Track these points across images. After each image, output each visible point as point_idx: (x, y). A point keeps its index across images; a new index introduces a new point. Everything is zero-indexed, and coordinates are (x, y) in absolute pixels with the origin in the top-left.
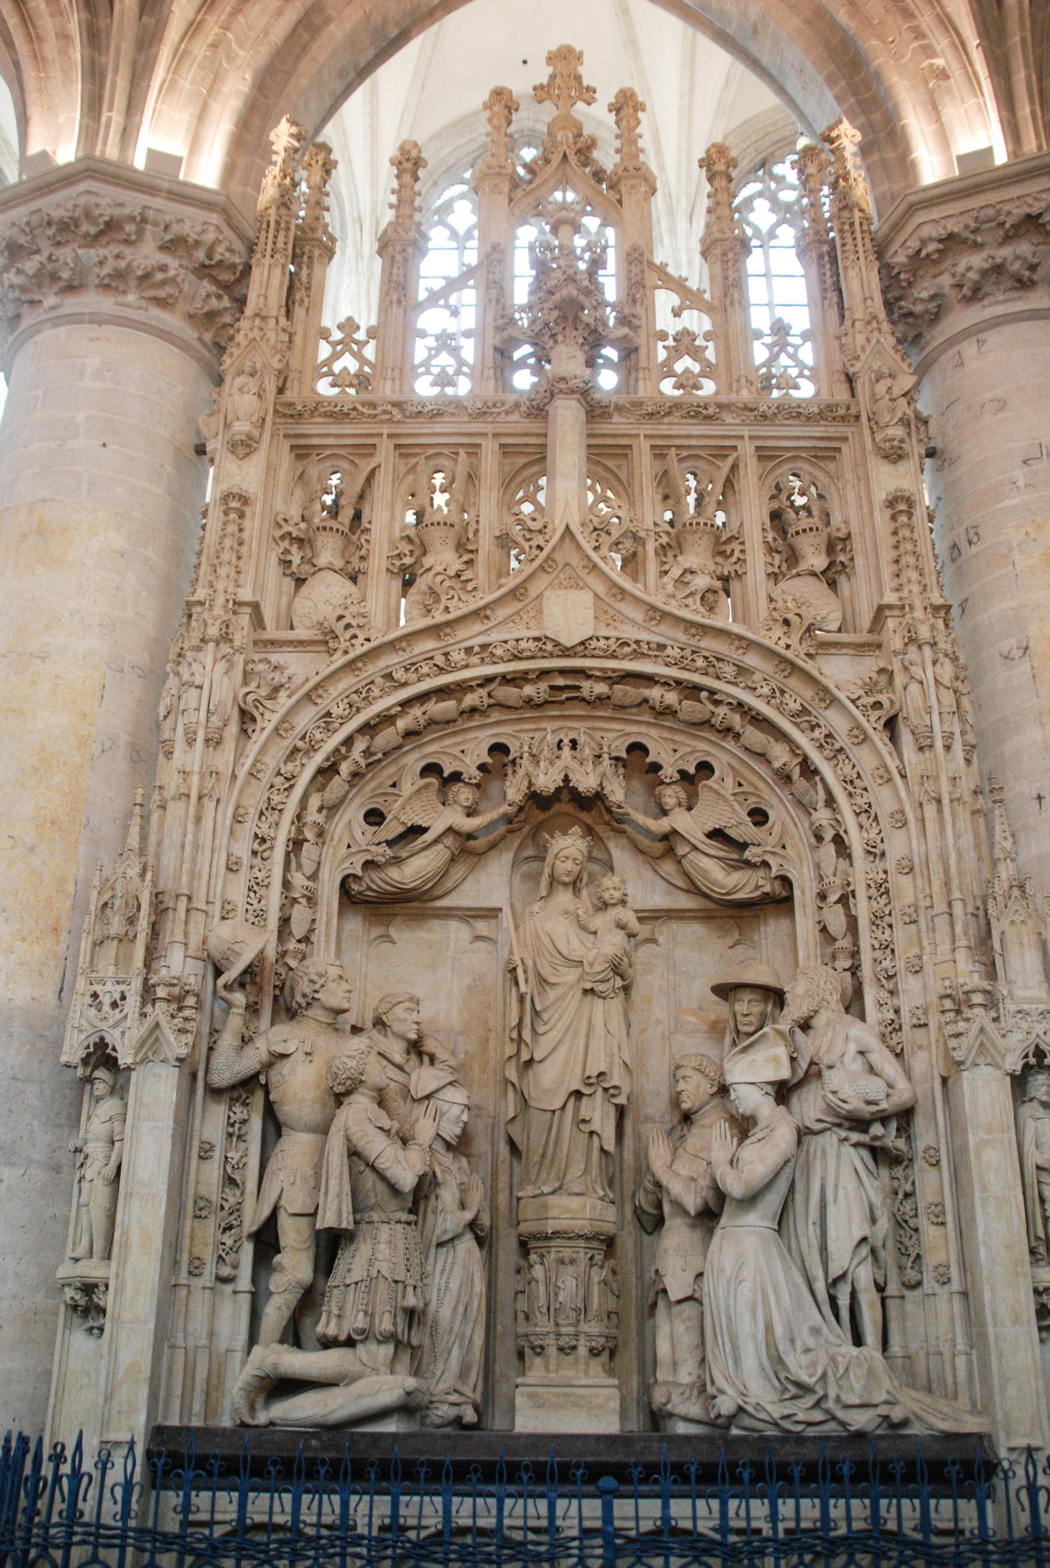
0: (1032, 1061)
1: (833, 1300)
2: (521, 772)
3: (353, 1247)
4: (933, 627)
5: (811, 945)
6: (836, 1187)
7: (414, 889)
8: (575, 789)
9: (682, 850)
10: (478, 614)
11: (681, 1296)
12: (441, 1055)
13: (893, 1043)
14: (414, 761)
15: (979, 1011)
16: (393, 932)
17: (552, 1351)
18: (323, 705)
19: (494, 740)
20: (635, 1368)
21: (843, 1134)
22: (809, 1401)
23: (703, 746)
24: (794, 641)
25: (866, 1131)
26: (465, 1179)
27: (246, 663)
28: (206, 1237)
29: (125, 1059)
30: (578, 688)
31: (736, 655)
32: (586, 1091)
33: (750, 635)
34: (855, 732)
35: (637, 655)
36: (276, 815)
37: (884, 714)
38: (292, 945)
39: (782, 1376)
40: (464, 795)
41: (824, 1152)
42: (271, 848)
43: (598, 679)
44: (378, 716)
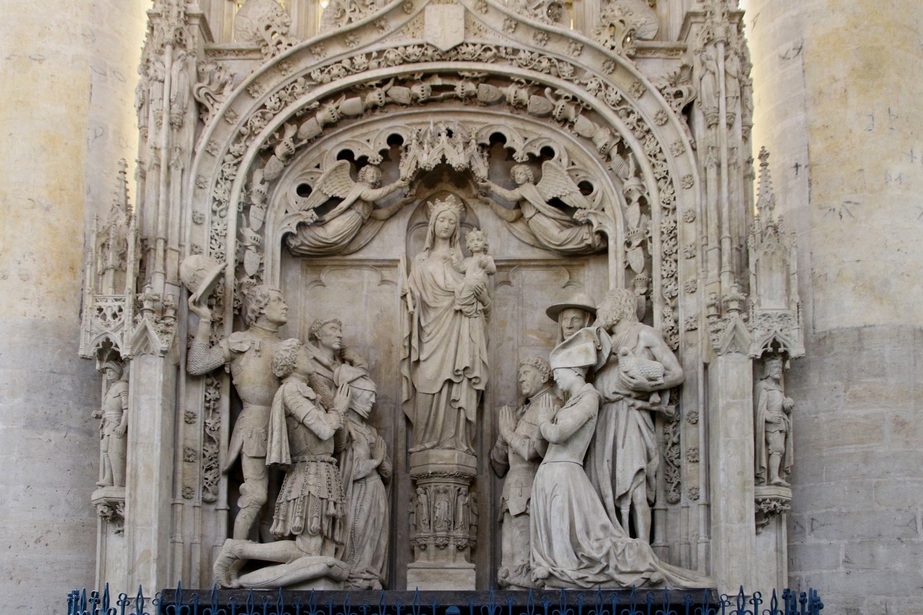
4: (727, 30)
5: (620, 279)
10: (374, 24)
11: (518, 512)
17: (432, 548)
18: (259, 98)
20: (488, 560)
24: (618, 43)
26: (374, 440)
27: (198, 64)
30: (452, 88)
31: (572, 57)
33: (584, 38)
34: (660, 116)
35: (497, 59)
37: (683, 101)
38: (245, 279)
41: (617, 414)
42: (227, 209)
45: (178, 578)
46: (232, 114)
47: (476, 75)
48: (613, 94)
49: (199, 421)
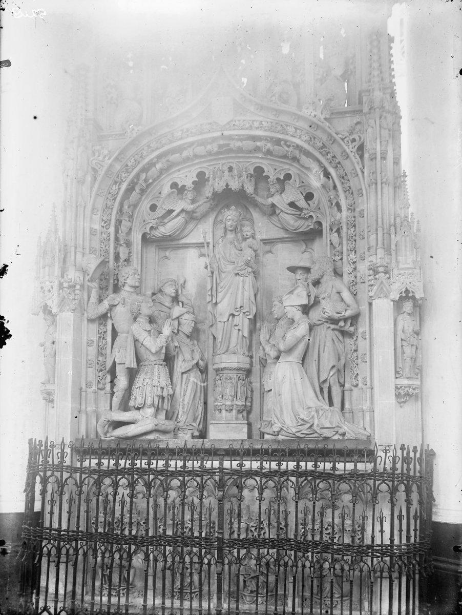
0: (404, 295)
1: (321, 390)
2: (210, 183)
3: (140, 374)
6: (325, 346)
7: (169, 236)
8: (231, 189)
9: (278, 212)
12: (186, 302)
13: (353, 290)
15: (382, 275)
16: (167, 253)
19: (199, 170)
21: (328, 325)
22: (308, 425)
23: (287, 167)
24: (318, 113)
25: (337, 324)
28: (92, 374)
29: (55, 310)
32: (237, 313)
36: (110, 211)
39: (297, 417)
42: (109, 224)
43: (238, 140)
45: (83, 432)
46: (110, 173)
47: (242, 137)
48: (318, 143)
49: (95, 344)
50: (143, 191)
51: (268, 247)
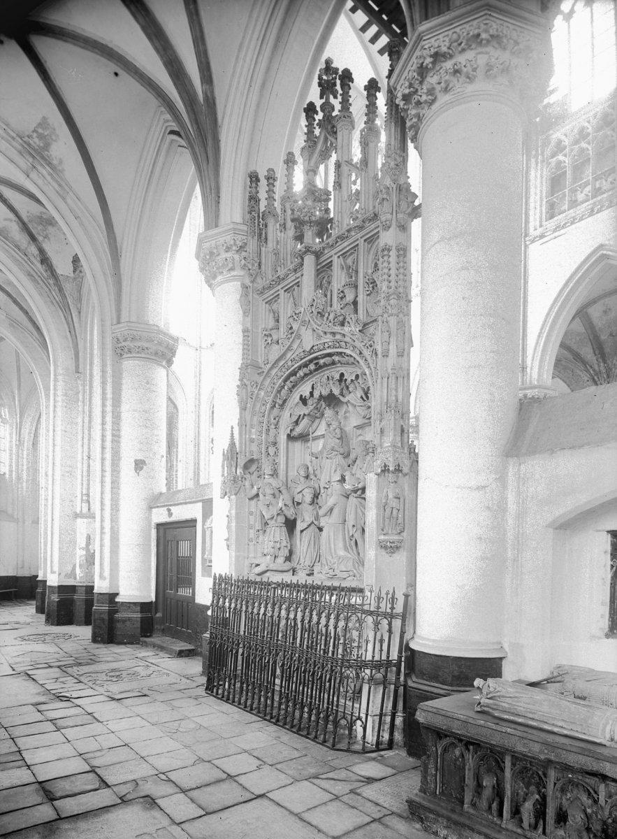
0: (383, 468)
14: (295, 397)
40: (310, 402)
44: (279, 387)
50: (282, 406)
51: (360, 432)
